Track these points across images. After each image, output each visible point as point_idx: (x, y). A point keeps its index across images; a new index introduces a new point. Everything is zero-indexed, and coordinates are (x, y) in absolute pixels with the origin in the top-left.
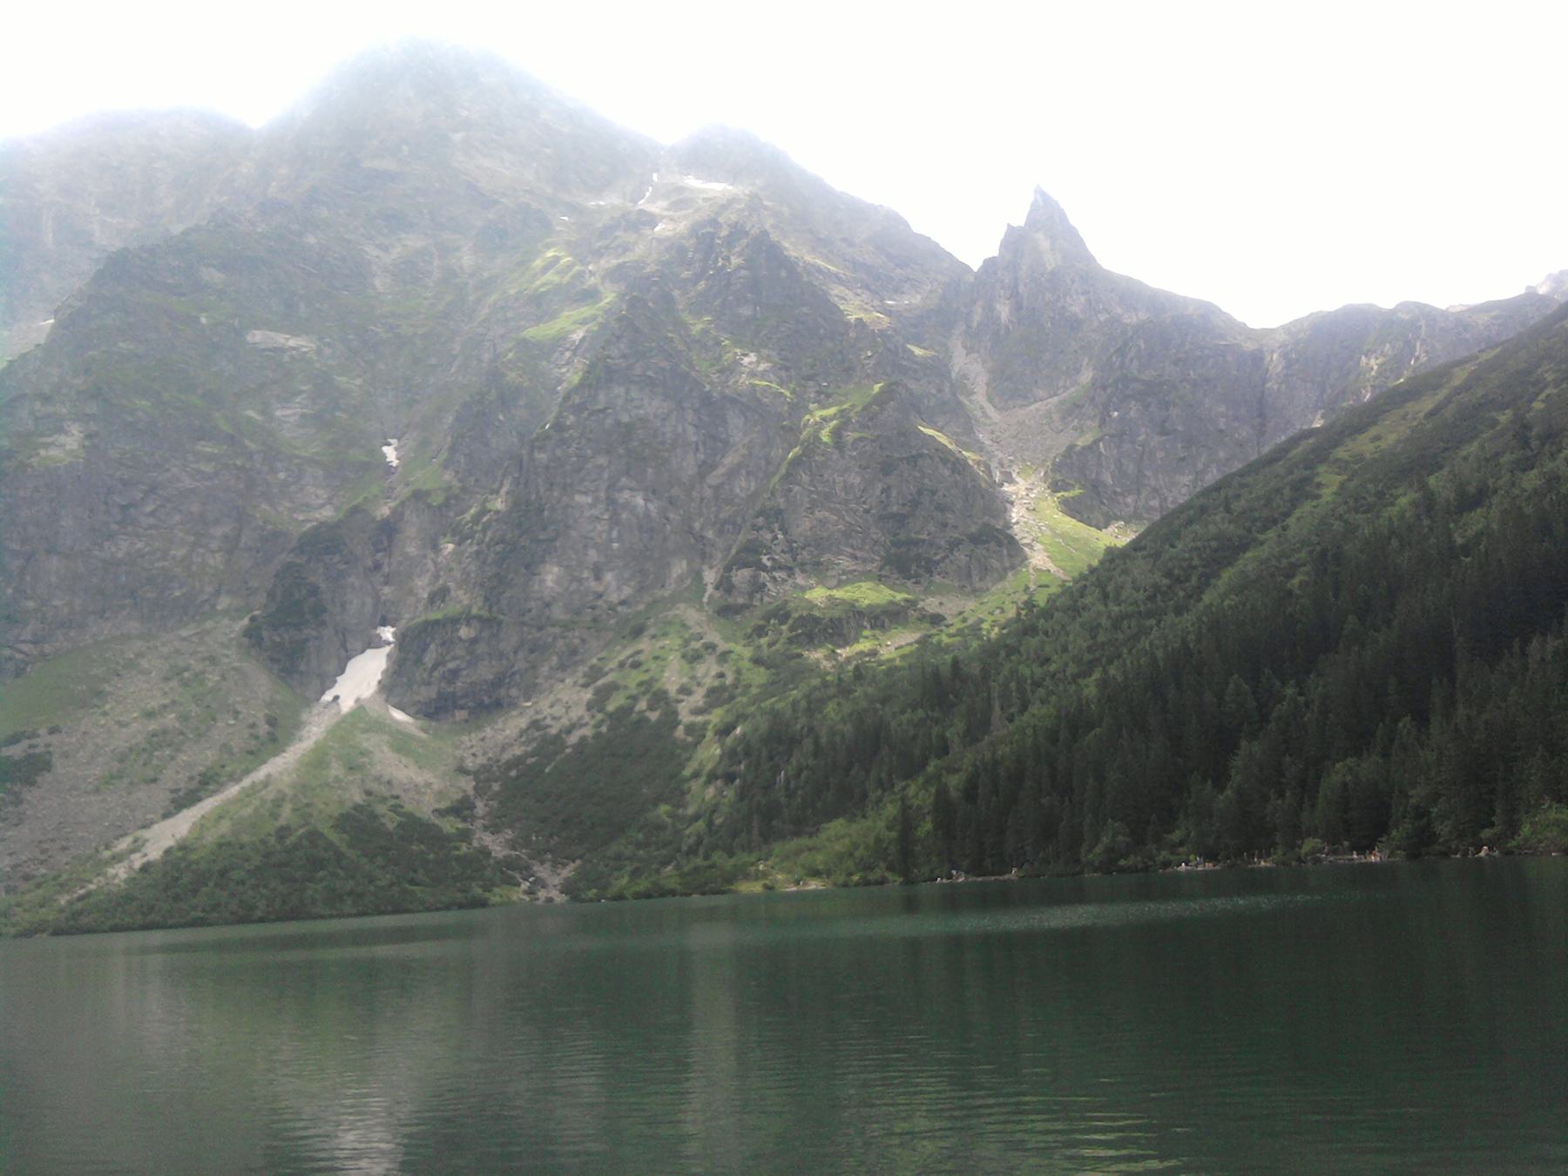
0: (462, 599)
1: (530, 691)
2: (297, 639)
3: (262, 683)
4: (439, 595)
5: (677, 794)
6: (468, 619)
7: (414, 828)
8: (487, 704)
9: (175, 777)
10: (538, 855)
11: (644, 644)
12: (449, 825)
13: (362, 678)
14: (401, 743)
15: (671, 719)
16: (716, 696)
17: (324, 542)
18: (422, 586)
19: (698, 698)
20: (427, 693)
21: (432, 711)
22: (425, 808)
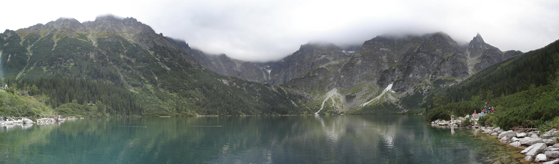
0: (401, 78)
1: (408, 89)
2: (382, 83)
3: (378, 88)
4: (399, 77)
5: (421, 102)
6: (401, 80)
7: (391, 104)
8: (403, 90)
9: (368, 98)
10: (404, 108)
11: (421, 84)
12: (395, 104)
13: (390, 87)
14: (392, 95)
15: (422, 93)
16: (428, 90)
17: (386, 71)
18: (397, 76)
19: (426, 90)
20: (396, 89)
21: (397, 91)
22: (393, 102)
